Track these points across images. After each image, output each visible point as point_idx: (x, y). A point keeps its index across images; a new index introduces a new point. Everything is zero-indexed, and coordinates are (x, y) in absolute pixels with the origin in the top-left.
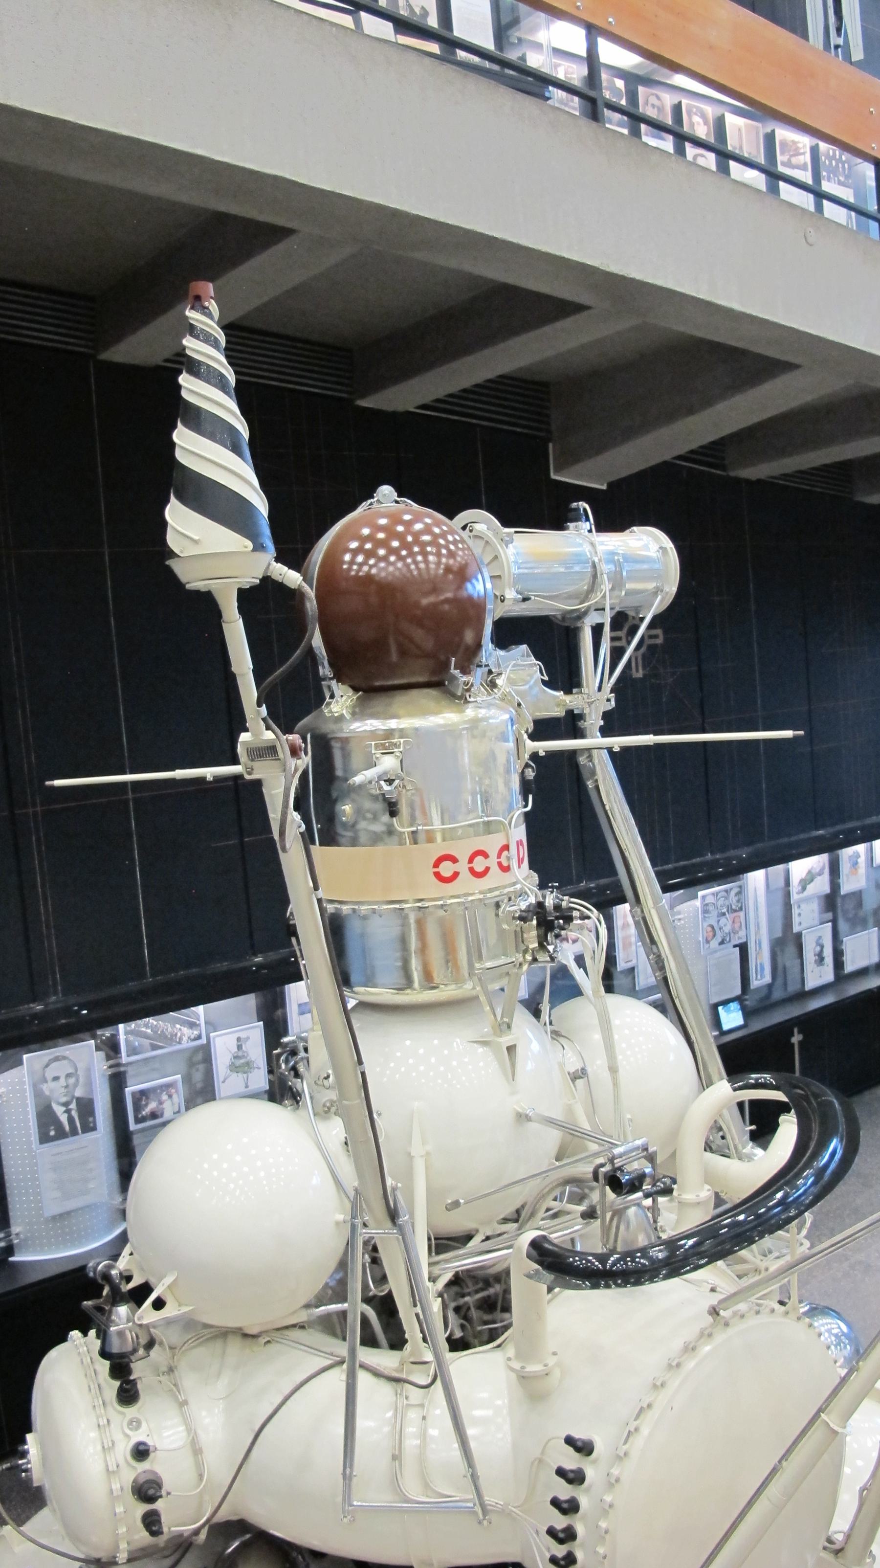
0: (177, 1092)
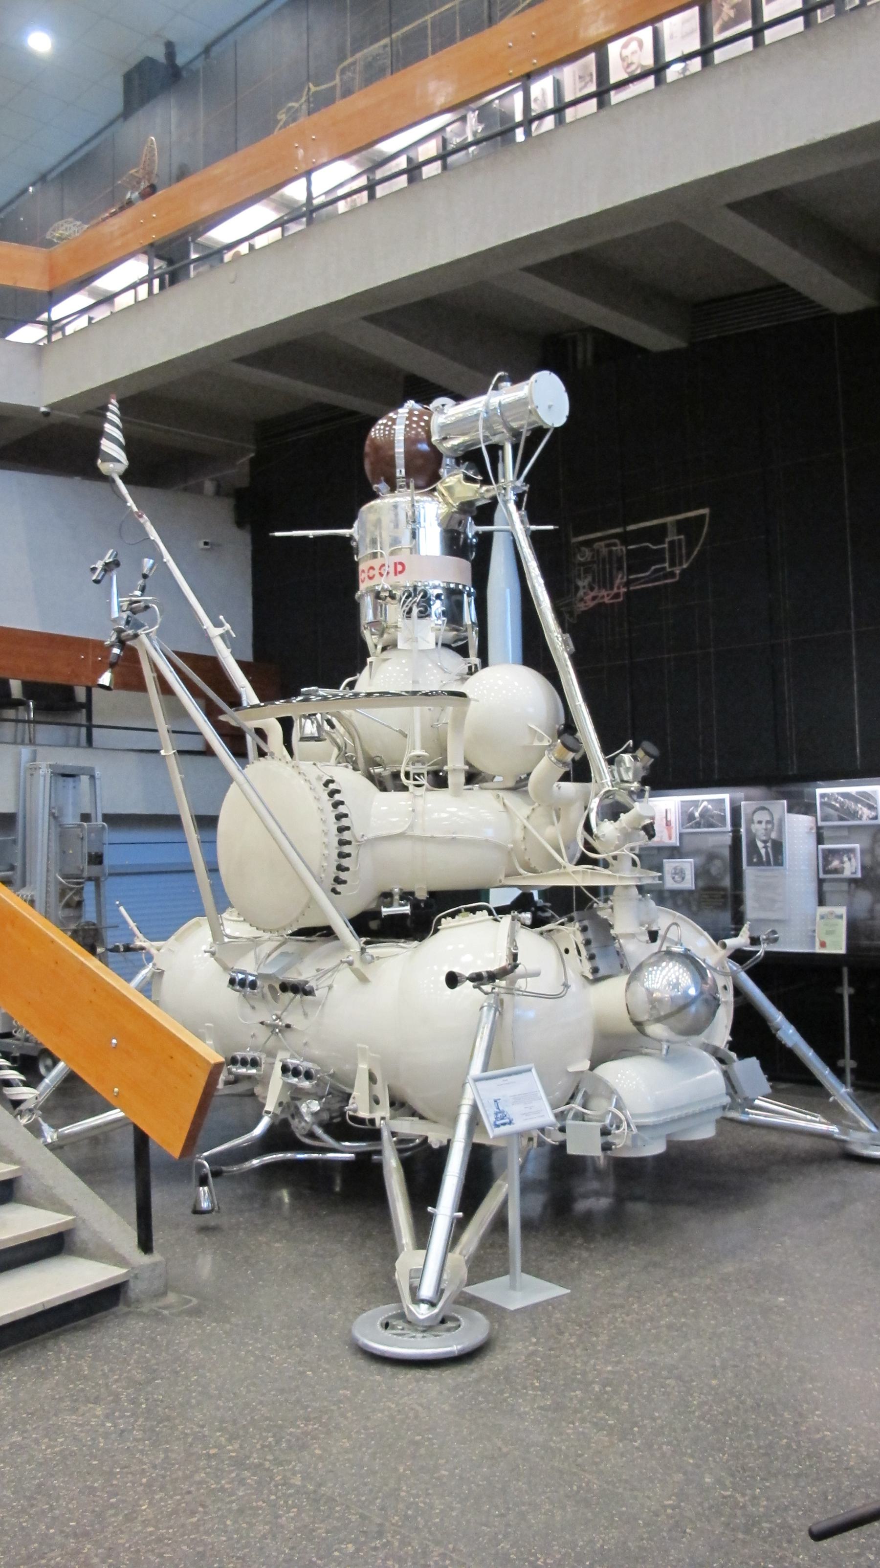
0: (855, 856)
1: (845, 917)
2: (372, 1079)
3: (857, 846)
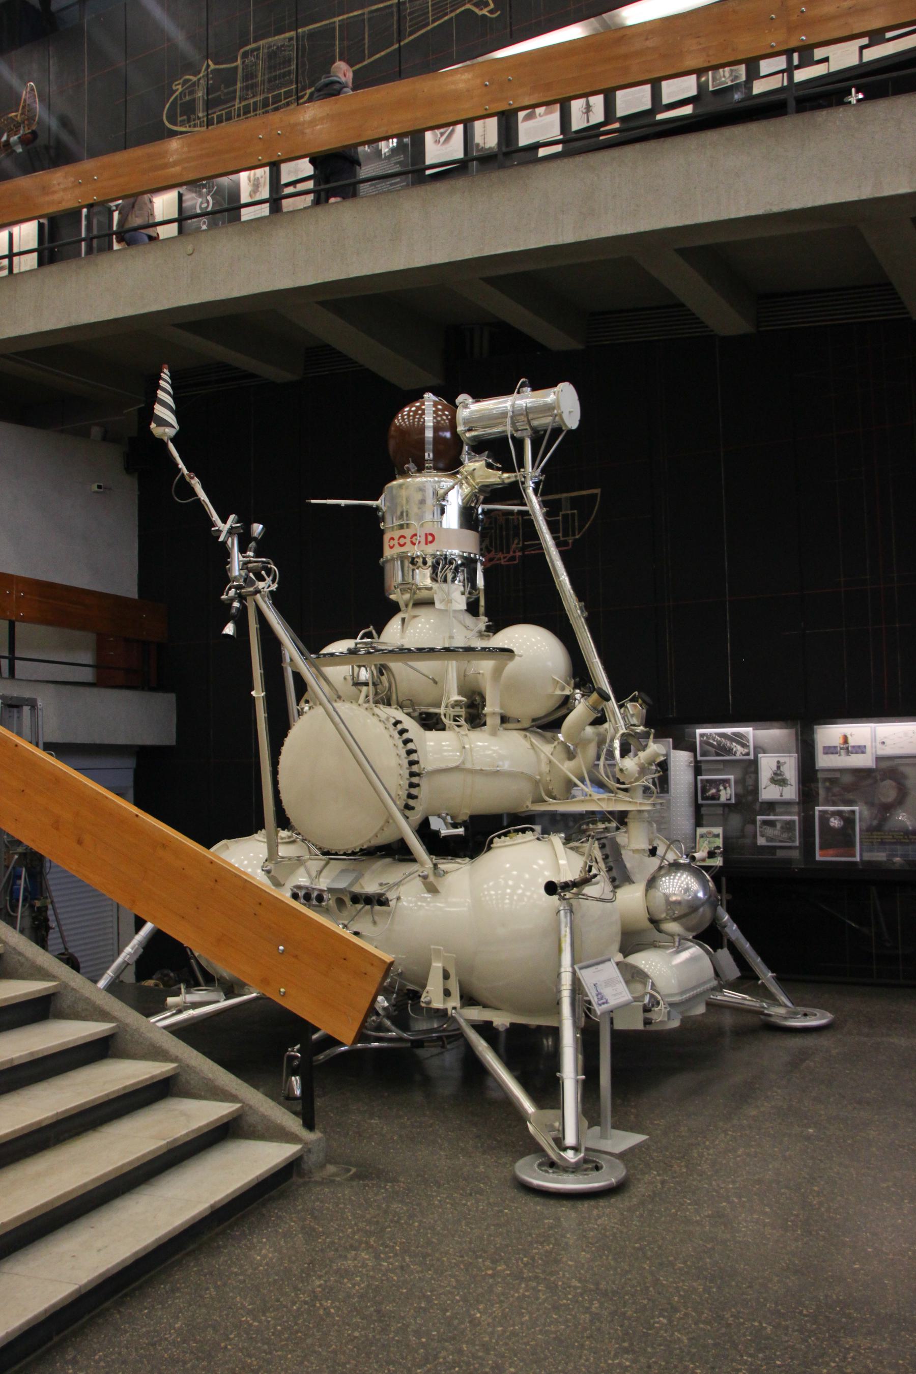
0: (730, 786)
1: (721, 836)
2: (446, 976)
3: (732, 777)
